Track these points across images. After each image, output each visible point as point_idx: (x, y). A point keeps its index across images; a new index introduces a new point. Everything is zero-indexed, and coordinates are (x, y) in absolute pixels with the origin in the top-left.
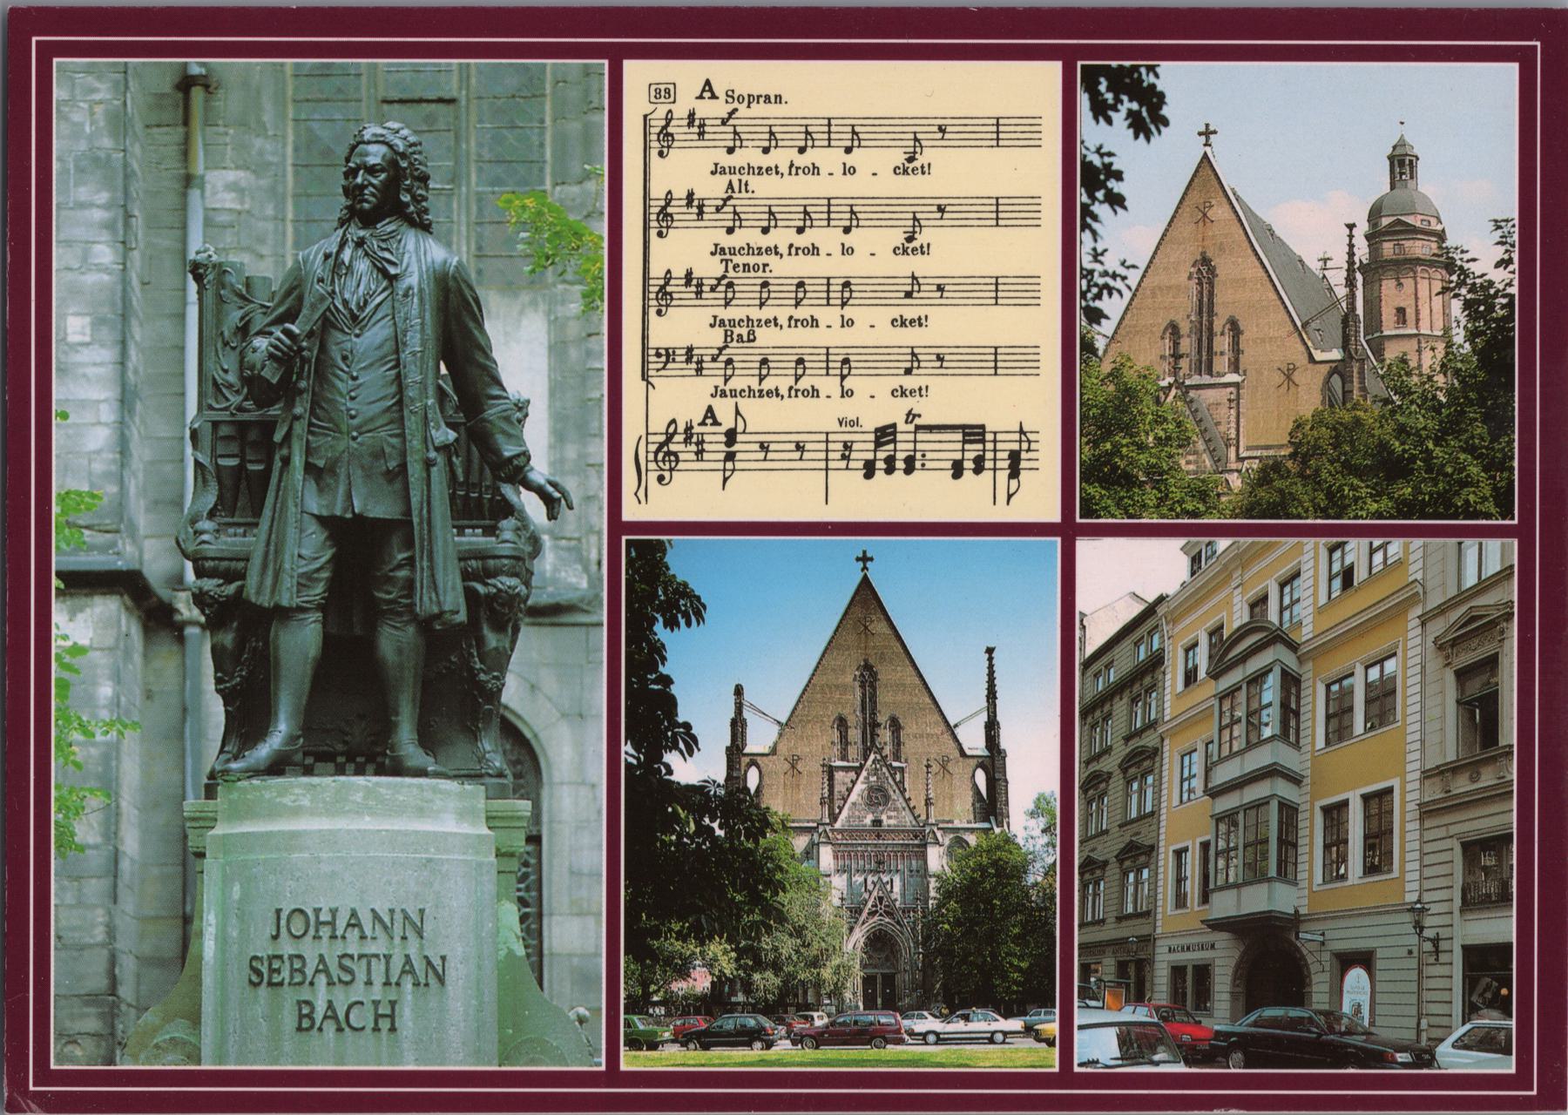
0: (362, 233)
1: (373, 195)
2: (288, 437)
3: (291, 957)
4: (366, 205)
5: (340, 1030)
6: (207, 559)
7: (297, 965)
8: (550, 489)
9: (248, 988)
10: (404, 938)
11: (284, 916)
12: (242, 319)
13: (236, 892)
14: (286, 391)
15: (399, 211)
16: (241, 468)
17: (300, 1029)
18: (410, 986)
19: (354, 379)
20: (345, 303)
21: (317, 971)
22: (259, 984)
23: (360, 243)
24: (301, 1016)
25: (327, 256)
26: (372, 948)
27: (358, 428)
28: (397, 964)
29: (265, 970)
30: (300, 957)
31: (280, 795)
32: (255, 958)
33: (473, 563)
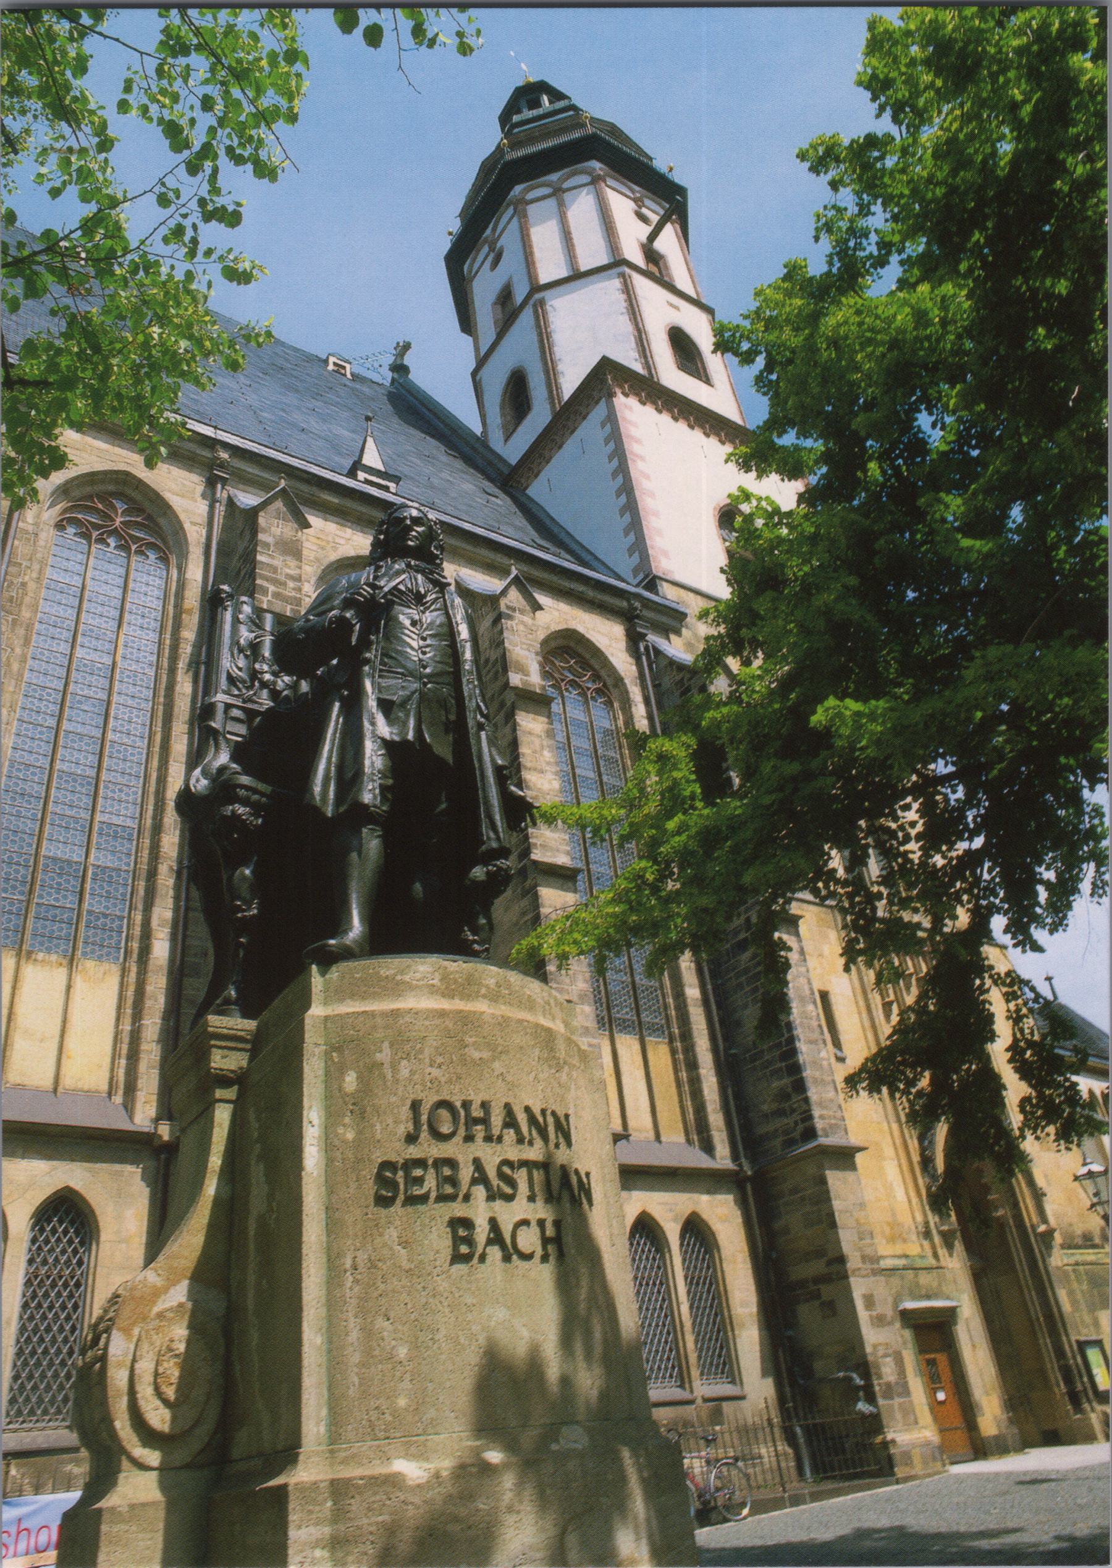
3: (439, 1163)
5: (507, 1258)
7: (447, 1171)
9: (373, 1209)
13: (350, 1081)
17: (457, 1258)
24: (457, 1241)
27: (429, 676)
30: (452, 1163)
31: (402, 972)
32: (386, 1165)
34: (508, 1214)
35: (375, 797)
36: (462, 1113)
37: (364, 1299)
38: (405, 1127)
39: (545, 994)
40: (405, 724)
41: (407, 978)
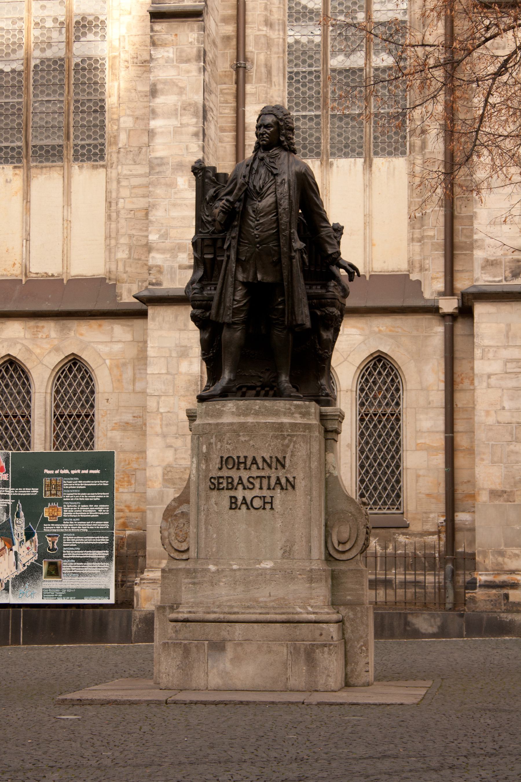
1: (267, 137)
3: (228, 478)
5: (248, 509)
6: (196, 301)
7: (230, 480)
9: (208, 492)
10: (276, 469)
11: (224, 459)
12: (215, 192)
14: (227, 226)
15: (279, 145)
16: (213, 260)
17: (231, 508)
18: (279, 490)
20: (254, 186)
21: (238, 484)
22: (214, 489)
24: (231, 503)
25: (247, 166)
26: (263, 474)
28: (273, 481)
29: (216, 482)
31: (223, 406)
32: (212, 478)
33: (315, 301)
34: (249, 495)
36: (236, 461)
37: (206, 520)
38: (218, 466)
41: (224, 409)
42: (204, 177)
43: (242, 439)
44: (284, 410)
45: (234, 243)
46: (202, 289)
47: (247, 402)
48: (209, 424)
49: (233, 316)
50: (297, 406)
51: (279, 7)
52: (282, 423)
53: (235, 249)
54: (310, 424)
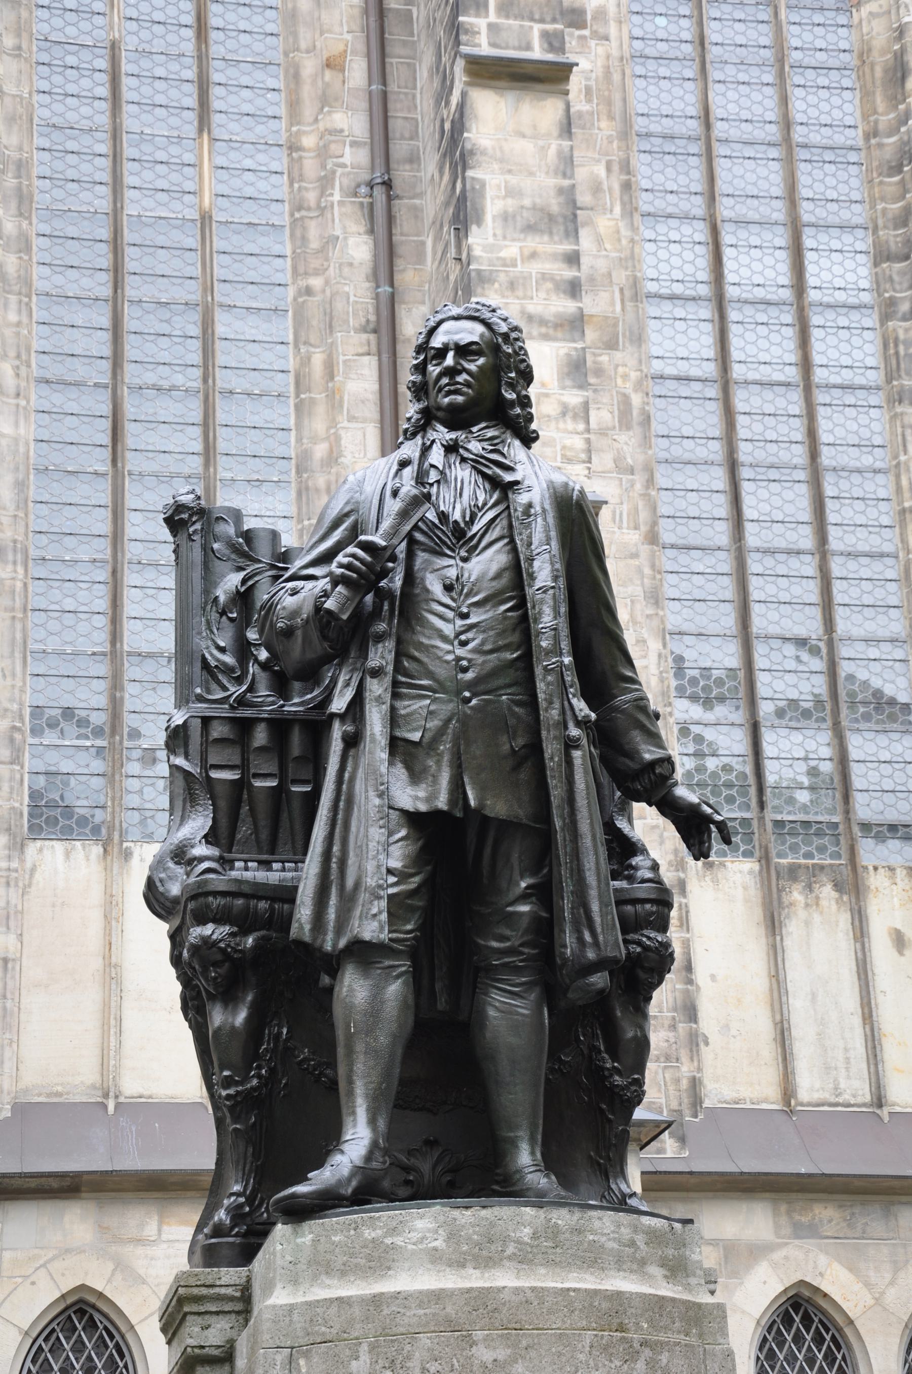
0: (453, 435)
1: (467, 384)
2: (357, 704)
4: (460, 399)
6: (215, 894)
8: (709, 810)
16: (240, 786)
19: (464, 616)
20: (443, 517)
23: (451, 448)
27: (470, 685)
31: (393, 1231)
35: (381, 928)
39: (626, 1232)
40: (435, 778)
41: (399, 1241)
42: (208, 533)
43: (484, 1354)
44: (615, 1246)
45: (376, 688)
46: (226, 862)
47: (484, 1213)
48: (339, 1299)
49: (390, 922)
50: (654, 1237)
51: (15, 516)
52: (619, 1294)
53: (385, 708)
54: (699, 1305)
